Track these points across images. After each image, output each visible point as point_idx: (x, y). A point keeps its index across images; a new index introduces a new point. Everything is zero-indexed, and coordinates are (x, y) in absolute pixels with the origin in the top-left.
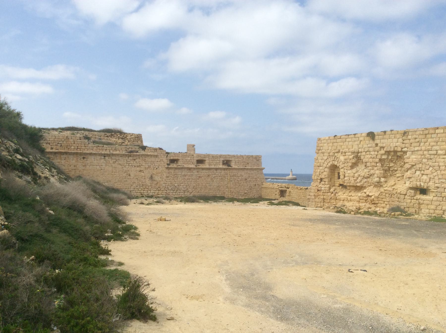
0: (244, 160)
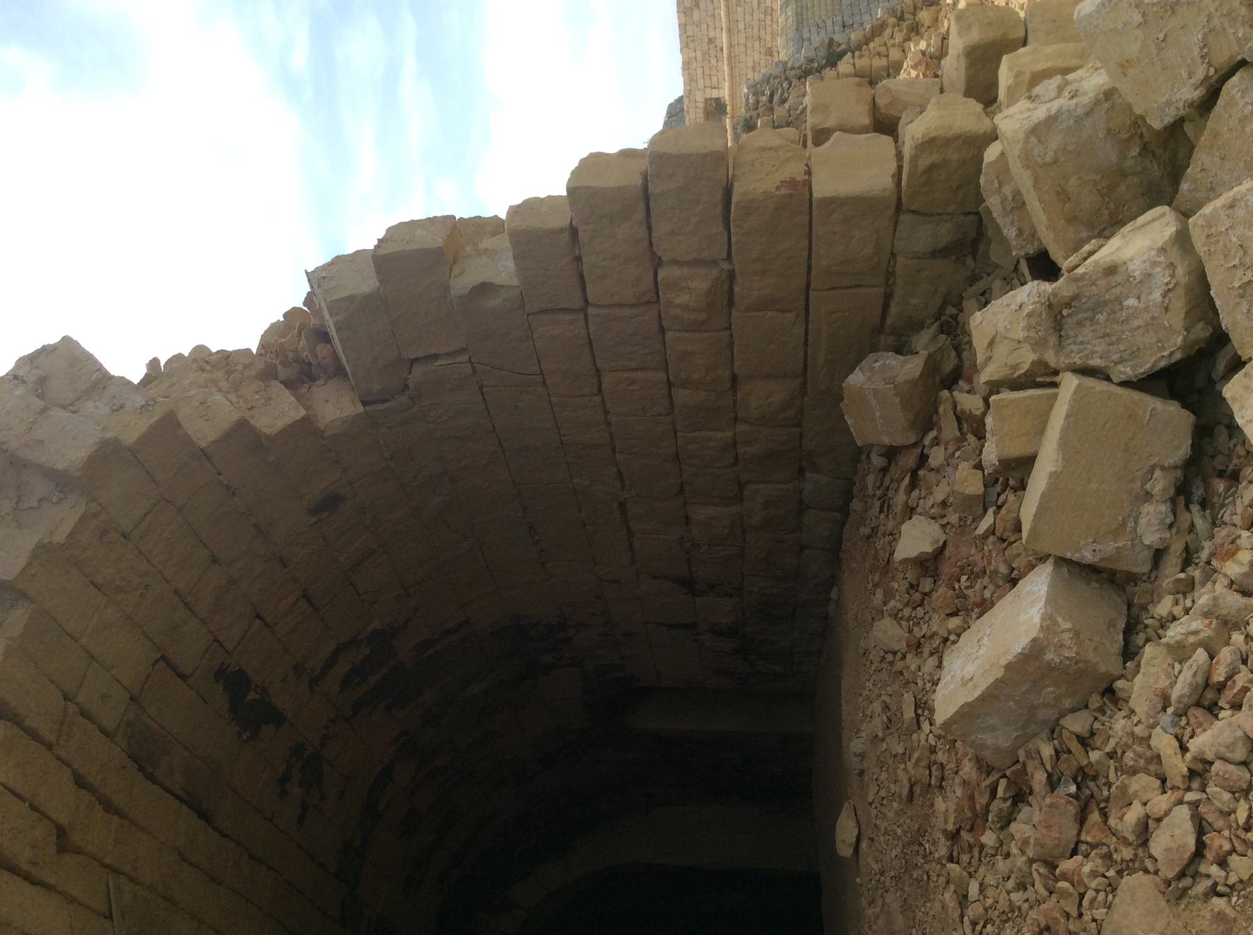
0: (699, 55)
